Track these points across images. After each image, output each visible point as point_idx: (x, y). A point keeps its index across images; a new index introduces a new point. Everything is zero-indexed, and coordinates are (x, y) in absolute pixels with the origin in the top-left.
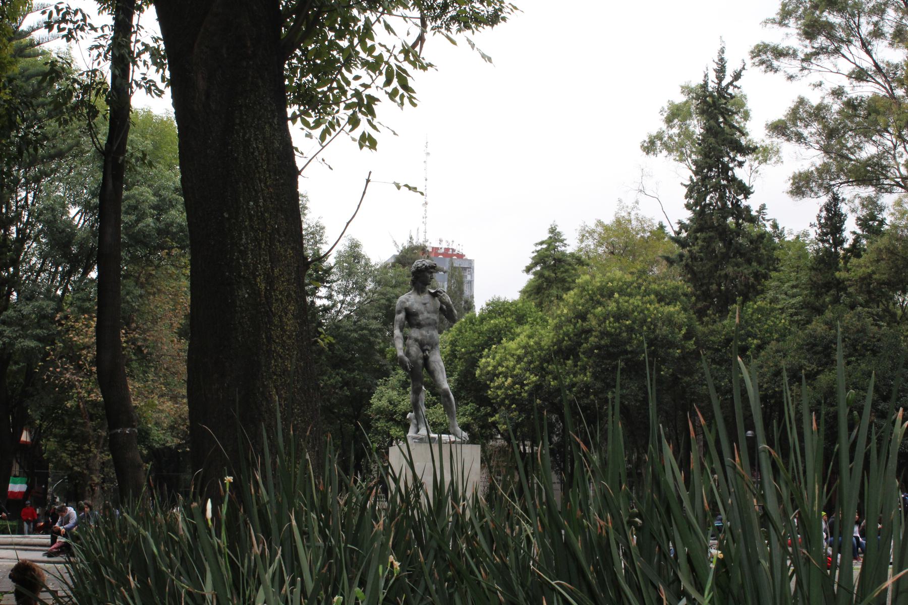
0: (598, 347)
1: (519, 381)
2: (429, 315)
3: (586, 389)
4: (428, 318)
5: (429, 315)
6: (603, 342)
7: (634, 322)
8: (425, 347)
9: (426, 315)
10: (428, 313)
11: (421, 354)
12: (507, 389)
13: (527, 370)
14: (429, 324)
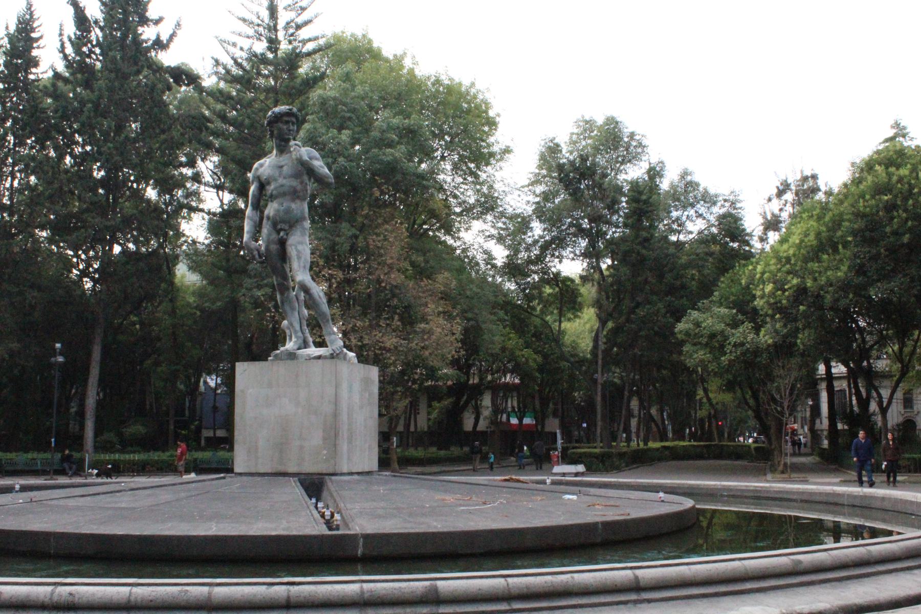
0: (854, 233)
1: (780, 286)
2: (284, 181)
3: (845, 287)
4: (282, 186)
5: (284, 181)
6: (856, 226)
7: (896, 196)
8: (279, 227)
9: (281, 181)
10: (285, 178)
11: (274, 236)
12: (769, 296)
13: (789, 273)
14: (284, 194)
